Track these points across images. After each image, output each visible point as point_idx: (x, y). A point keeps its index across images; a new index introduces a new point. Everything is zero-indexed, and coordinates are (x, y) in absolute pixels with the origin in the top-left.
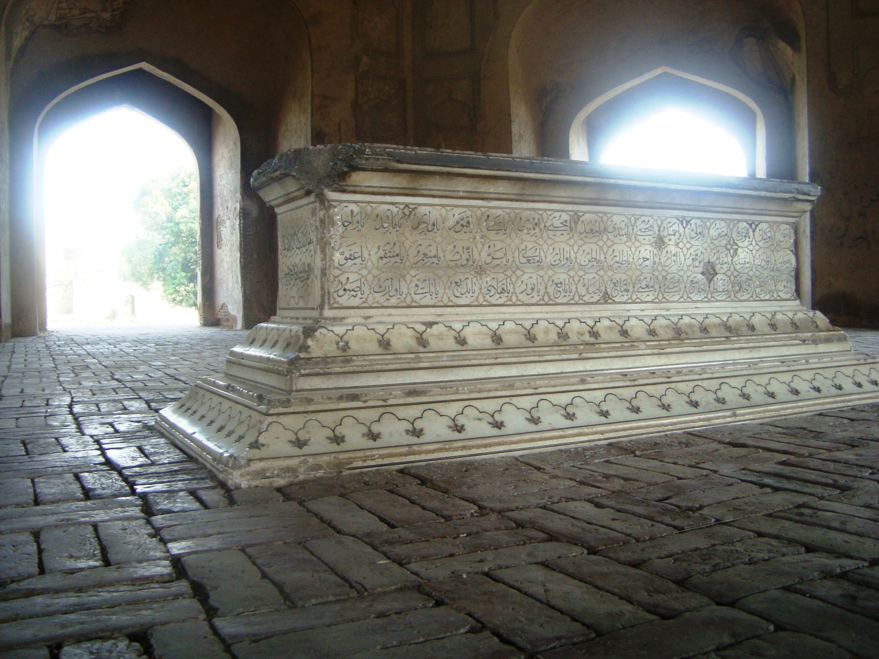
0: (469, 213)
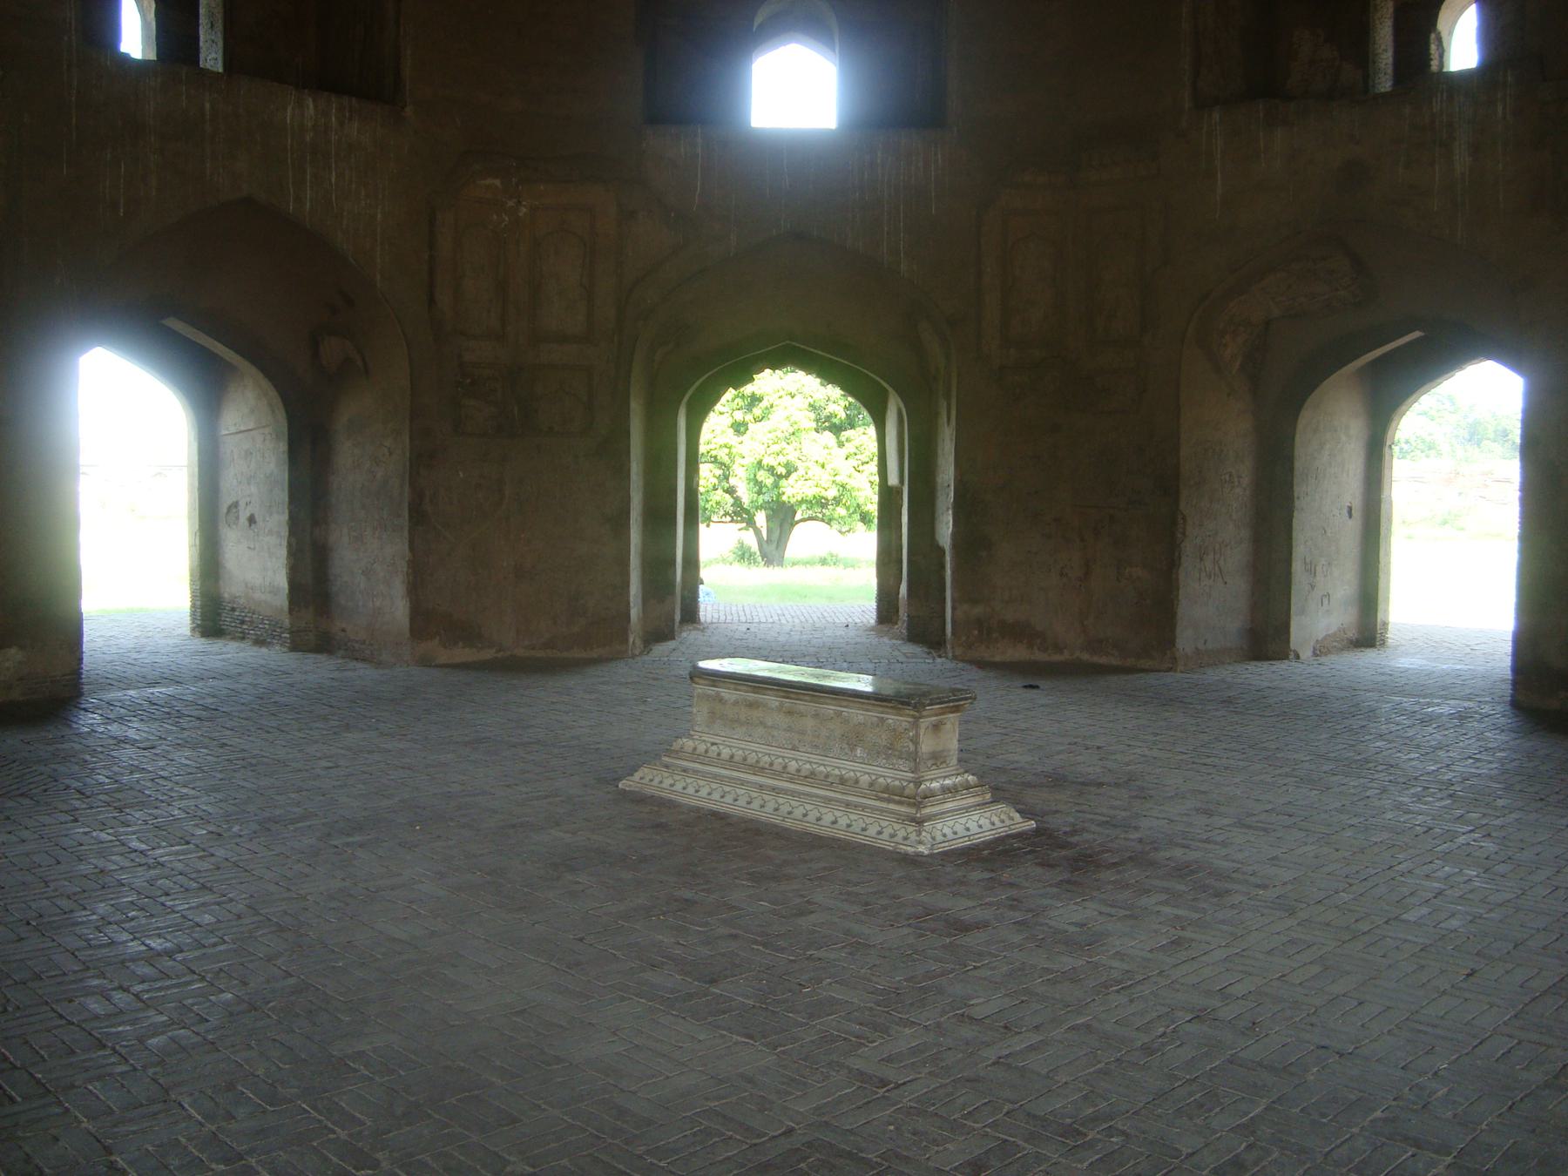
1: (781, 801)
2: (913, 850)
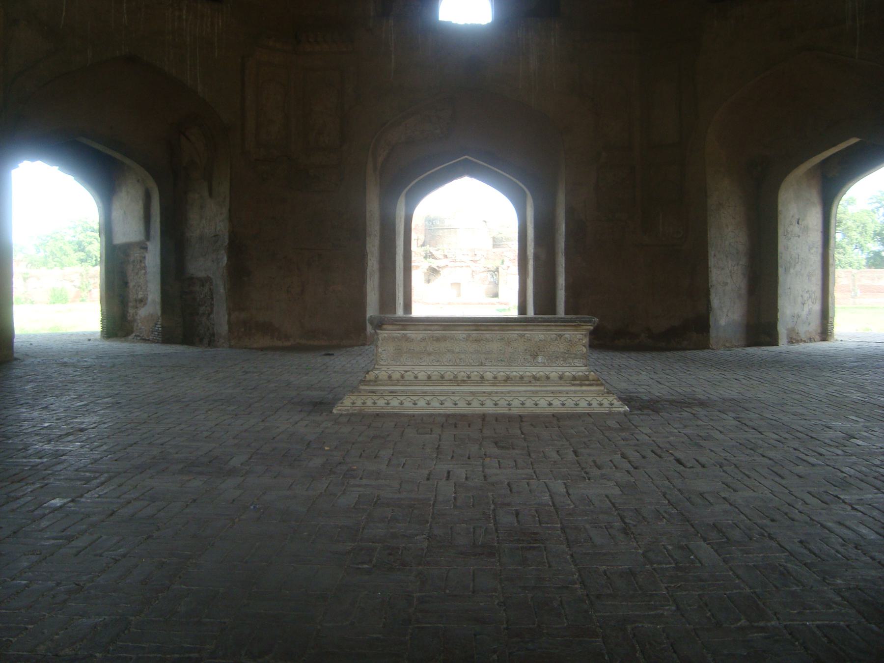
1: (495, 398)
2: (623, 409)
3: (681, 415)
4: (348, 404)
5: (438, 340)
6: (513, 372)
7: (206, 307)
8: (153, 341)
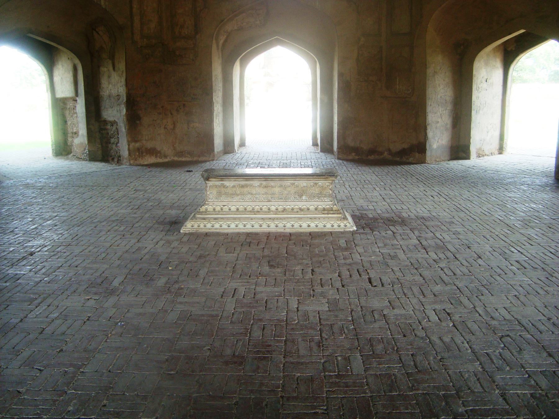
0: (235, 184)
1: (276, 222)
2: (352, 229)
3: (386, 234)
4: (189, 226)
5: (243, 186)
6: (288, 205)
7: (115, 139)
8: (84, 160)
